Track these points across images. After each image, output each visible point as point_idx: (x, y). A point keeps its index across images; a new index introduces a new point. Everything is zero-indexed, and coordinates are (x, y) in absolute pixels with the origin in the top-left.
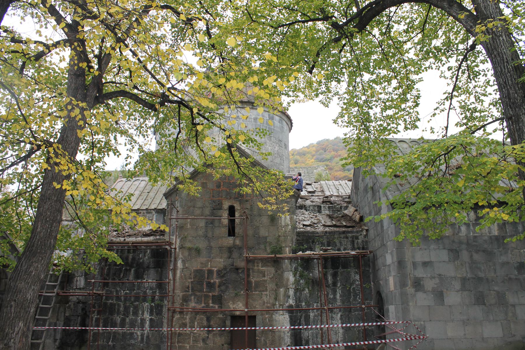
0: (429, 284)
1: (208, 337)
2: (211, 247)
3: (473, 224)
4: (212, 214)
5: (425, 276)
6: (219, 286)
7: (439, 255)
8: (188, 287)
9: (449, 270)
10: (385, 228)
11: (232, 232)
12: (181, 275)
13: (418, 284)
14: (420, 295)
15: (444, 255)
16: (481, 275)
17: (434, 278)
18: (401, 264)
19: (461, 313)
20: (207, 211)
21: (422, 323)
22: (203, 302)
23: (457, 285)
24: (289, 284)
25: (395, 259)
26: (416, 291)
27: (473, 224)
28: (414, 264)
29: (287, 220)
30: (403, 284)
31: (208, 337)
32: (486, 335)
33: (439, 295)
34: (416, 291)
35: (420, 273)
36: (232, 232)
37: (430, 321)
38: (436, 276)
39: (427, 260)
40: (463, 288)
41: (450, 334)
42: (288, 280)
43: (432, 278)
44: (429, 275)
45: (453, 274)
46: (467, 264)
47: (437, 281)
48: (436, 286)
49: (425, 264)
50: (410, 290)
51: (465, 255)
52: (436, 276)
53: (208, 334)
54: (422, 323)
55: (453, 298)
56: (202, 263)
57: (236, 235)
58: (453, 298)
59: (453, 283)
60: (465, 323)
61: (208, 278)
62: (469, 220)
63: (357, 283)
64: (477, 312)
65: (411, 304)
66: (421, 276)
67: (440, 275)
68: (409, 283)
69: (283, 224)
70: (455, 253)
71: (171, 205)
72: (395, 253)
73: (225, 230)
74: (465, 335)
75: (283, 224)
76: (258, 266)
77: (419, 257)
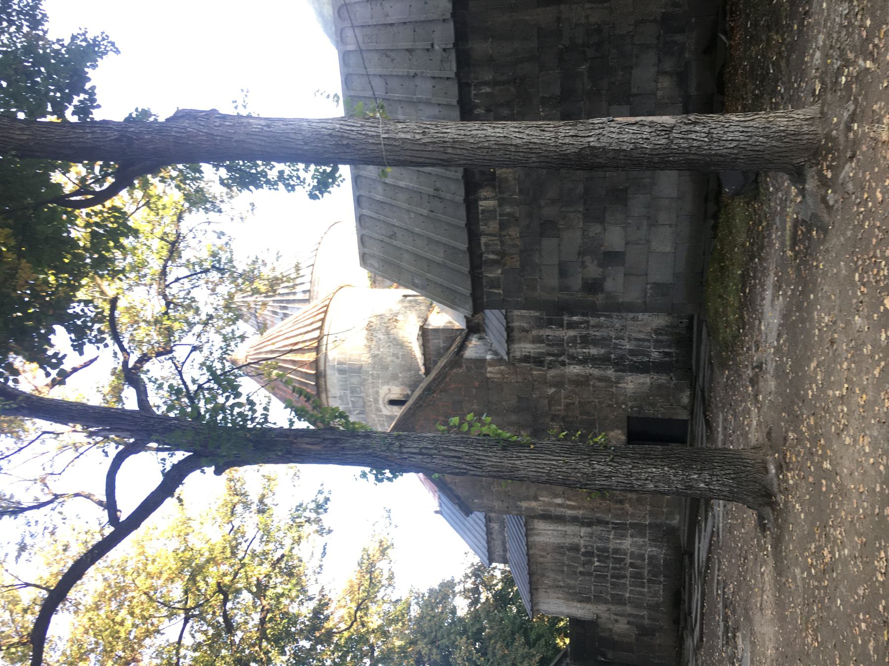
0: (593, 270)
3: (500, 192)
5: (580, 276)
7: (550, 251)
9: (572, 239)
13: (593, 286)
14: (609, 285)
15: (549, 244)
16: (580, 189)
17: (583, 263)
19: (638, 229)
21: (649, 286)
23: (595, 229)
27: (500, 192)
28: (564, 288)
32: (675, 194)
33: (612, 258)
34: (602, 291)
35: (576, 283)
38: (580, 260)
39: (556, 271)
40: (600, 219)
41: (668, 249)
42: (578, 375)
43: (583, 265)
44: (580, 270)
45: (579, 233)
46: (563, 209)
47: (588, 259)
48: (596, 262)
49: (563, 272)
50: (600, 299)
51: (549, 212)
52: (580, 260)
54: (649, 286)
55: (614, 237)
58: (614, 237)
59: (591, 235)
60: (653, 223)
62: (493, 198)
64: (637, 204)
65: (621, 300)
66: (580, 282)
67: (579, 254)
68: (590, 298)
70: (548, 228)
71: (480, 508)
74: (671, 226)
76: (559, 410)
77: (553, 280)
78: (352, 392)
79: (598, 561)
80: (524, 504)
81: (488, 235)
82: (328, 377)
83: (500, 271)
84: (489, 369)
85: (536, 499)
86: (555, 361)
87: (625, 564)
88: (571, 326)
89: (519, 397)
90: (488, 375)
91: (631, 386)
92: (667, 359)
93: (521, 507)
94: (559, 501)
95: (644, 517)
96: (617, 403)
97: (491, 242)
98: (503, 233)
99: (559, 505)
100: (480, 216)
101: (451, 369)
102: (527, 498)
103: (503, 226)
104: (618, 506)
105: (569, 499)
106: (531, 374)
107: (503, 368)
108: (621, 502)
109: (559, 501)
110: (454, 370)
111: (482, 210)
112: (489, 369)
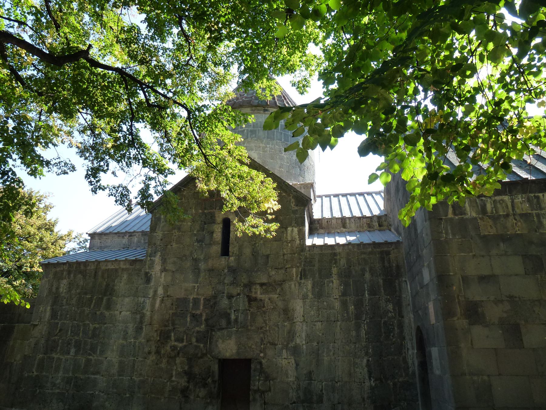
0: (494, 313)
1: (188, 387)
2: (199, 269)
4: (203, 229)
5: (484, 299)
6: (206, 320)
8: (168, 321)
10: (419, 231)
11: (225, 252)
12: (160, 305)
14: (478, 331)
15: (516, 264)
17: (502, 301)
18: (443, 279)
20: (197, 227)
21: (486, 378)
22: (185, 341)
24: (296, 316)
25: (434, 274)
26: (471, 324)
29: (294, 234)
30: (447, 313)
31: (188, 387)
34: (471, 324)
35: (476, 293)
36: (225, 252)
37: (500, 375)
39: (486, 272)
43: (497, 302)
44: (492, 298)
48: (505, 315)
50: (460, 322)
53: (188, 382)
54: (486, 378)
56: (186, 290)
57: (230, 254)
61: (192, 309)
63: (390, 315)
65: (462, 345)
66: (477, 298)
68: (458, 310)
69: (289, 239)
72: (432, 265)
73: (217, 249)
75: (289, 239)
77: (473, 268)
78: (251, 131)
79: (95, 328)
80: (157, 259)
81: (513, 202)
82: (264, 115)
83: (474, 215)
84: (296, 230)
85: (164, 270)
86: (307, 289)
87: (90, 355)
88: (344, 304)
89: (268, 256)
90: (290, 229)
91: (284, 362)
92: (315, 398)
93: (154, 257)
94: (160, 291)
95: (141, 375)
96: (265, 349)
97: (504, 205)
98: (518, 218)
99: (155, 292)
100: (532, 195)
101: (294, 197)
102: (164, 261)
103: (525, 216)
104: (154, 349)
105: (162, 301)
106: (292, 267)
107: (298, 242)
108: (158, 352)
109: (160, 291)
110: (293, 200)
111: (538, 198)
112: (296, 230)
